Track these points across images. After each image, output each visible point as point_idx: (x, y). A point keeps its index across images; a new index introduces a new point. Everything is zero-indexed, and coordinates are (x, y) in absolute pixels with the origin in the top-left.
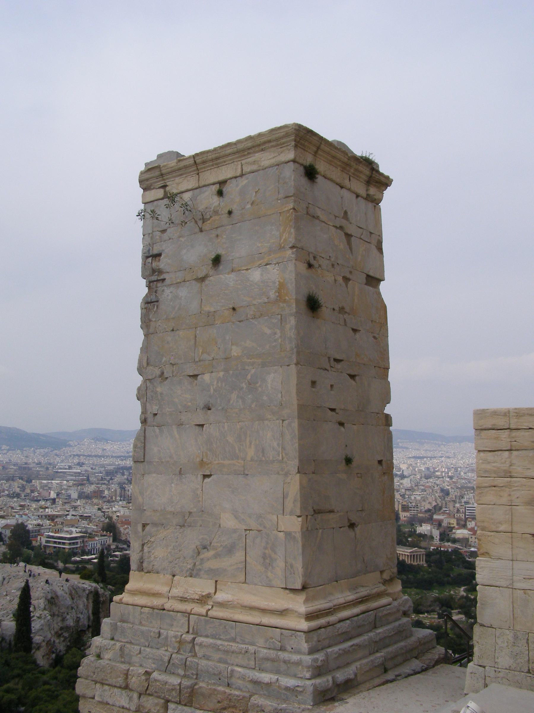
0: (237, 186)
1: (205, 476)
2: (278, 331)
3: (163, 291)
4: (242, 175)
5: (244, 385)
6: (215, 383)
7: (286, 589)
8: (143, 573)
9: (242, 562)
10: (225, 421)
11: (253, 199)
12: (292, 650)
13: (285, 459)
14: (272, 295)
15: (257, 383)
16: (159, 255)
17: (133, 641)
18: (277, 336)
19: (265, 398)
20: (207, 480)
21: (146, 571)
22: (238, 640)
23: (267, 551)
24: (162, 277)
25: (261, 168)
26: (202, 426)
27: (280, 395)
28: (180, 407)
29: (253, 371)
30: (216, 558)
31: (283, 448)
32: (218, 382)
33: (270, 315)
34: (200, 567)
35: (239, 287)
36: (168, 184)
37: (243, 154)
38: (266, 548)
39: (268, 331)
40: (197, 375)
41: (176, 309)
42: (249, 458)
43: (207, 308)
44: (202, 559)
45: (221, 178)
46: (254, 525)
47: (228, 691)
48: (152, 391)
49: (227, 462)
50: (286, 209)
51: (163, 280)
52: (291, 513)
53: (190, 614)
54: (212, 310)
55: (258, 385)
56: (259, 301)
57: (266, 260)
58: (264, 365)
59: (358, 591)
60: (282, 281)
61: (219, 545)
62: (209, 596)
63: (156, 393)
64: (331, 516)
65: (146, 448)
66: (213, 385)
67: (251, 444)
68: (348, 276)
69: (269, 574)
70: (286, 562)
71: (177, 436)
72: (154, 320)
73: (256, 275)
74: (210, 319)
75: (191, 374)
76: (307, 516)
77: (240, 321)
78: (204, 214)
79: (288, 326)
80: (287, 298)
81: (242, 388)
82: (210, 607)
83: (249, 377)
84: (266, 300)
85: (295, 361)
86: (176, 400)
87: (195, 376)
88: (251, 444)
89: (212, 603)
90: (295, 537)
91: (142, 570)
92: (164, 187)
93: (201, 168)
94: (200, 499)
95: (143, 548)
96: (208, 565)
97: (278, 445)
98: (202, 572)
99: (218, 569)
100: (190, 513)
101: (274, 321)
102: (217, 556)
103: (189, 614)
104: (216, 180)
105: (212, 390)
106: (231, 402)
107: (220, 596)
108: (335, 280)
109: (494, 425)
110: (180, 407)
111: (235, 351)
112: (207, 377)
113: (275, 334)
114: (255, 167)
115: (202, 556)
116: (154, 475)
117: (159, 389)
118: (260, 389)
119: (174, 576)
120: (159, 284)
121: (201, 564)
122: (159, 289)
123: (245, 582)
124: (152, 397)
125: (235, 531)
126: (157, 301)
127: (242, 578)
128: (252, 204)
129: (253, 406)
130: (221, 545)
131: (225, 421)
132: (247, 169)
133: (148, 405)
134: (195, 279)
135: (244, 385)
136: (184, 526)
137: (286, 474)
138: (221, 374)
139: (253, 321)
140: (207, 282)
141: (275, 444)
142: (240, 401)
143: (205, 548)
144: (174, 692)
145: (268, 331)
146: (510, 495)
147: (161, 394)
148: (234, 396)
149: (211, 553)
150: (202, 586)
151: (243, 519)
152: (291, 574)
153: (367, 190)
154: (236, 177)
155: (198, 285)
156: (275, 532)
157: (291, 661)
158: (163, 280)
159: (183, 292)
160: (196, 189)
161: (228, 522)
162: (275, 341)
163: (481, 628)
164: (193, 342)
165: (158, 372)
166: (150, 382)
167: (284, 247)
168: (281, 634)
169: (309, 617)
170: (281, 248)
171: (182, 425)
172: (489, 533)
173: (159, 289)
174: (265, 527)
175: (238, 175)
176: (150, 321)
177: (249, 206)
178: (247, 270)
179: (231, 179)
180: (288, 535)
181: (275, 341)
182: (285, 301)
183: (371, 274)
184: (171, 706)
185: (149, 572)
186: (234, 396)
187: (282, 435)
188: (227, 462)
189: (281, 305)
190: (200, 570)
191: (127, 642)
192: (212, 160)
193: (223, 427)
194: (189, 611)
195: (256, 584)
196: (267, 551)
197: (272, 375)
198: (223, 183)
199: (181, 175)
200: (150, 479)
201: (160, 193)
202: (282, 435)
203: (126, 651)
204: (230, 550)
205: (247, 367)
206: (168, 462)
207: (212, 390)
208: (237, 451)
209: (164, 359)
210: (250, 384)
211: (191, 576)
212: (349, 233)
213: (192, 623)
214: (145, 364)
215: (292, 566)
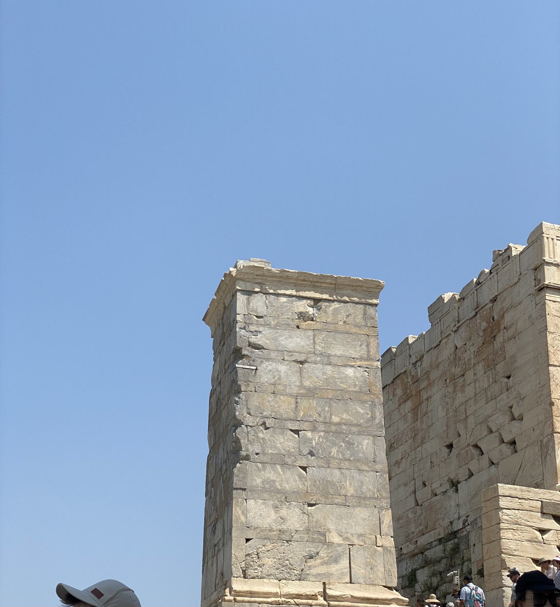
1: (310, 505)
6: (317, 439)
7: (385, 587)
9: (347, 568)
11: (345, 319)
19: (361, 455)
20: (310, 508)
23: (368, 560)
30: (323, 565)
34: (308, 572)
38: (368, 558)
39: (362, 411)
41: (276, 378)
43: (307, 383)
44: (310, 567)
46: (356, 541)
48: (254, 435)
52: (387, 535)
55: (355, 446)
56: (354, 390)
61: (325, 555)
63: (258, 437)
66: (315, 440)
69: (371, 576)
73: (350, 372)
81: (342, 446)
86: (279, 445)
87: (297, 432)
90: (390, 551)
96: (314, 571)
100: (297, 531)
106: (332, 454)
112: (309, 434)
113: (368, 414)
117: (261, 435)
119: (279, 581)
123: (351, 582)
125: (340, 545)
127: (348, 580)
128: (345, 322)
130: (327, 556)
136: (291, 541)
137: (381, 508)
140: (306, 365)
142: (340, 454)
143: (311, 557)
145: (362, 411)
147: (263, 439)
148: (334, 451)
149: (319, 561)
152: (389, 576)
159: (283, 368)
164: (293, 406)
174: (365, 543)
182: (374, 394)
185: (253, 578)
189: (372, 396)
190: (308, 574)
196: (368, 560)
197: (366, 441)
198: (320, 300)
200: (251, 502)
204: (336, 560)
215: (389, 570)
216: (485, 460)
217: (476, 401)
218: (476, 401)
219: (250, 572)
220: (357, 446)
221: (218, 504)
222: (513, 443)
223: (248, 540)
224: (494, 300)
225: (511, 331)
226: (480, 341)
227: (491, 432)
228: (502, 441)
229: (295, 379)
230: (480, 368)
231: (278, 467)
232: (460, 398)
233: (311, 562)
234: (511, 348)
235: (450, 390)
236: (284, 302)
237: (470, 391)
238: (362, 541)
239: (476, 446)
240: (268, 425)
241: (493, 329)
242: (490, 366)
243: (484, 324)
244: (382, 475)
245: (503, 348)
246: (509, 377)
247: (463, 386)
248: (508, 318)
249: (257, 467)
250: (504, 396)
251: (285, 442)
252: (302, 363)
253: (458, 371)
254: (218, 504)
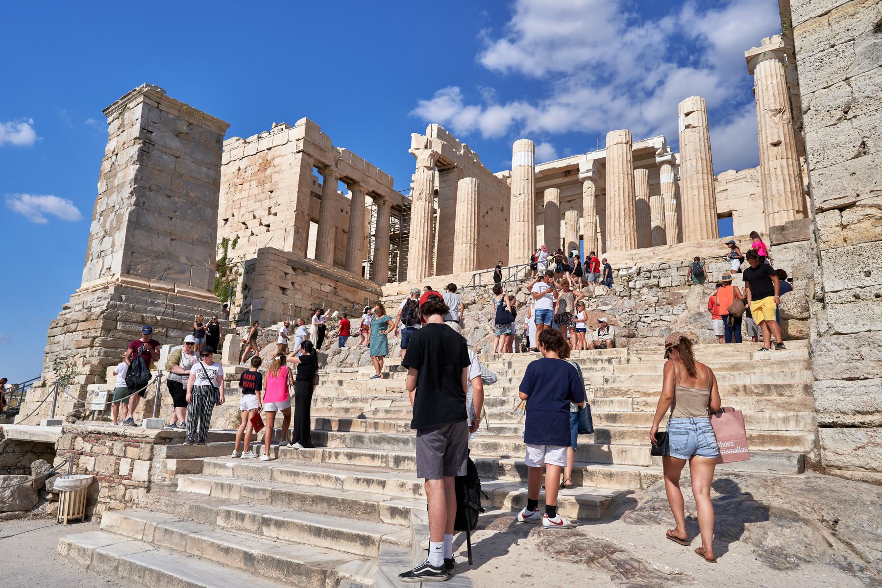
1: (172, 240)
74: (180, 176)
92: (158, 103)
102: (176, 273)
103: (167, 295)
111: (192, 194)
112: (177, 199)
117: (148, 193)
149: (171, 272)
159: (165, 157)
186: (190, 211)
201: (156, 105)
204: (183, 272)
214: (139, 177)
216: (248, 232)
217: (248, 200)
218: (248, 200)
219: (131, 272)
221: (108, 226)
222: (268, 226)
223: (132, 253)
224: (269, 149)
225: (277, 169)
226: (257, 169)
227: (254, 217)
228: (261, 224)
229: (172, 166)
230: (254, 183)
231: (156, 214)
232: (238, 196)
233: (168, 272)
234: (275, 177)
235: (232, 190)
237: (245, 194)
239: (244, 223)
241: (265, 165)
242: (261, 183)
243: (261, 161)
245: (271, 176)
246: (271, 192)
247: (241, 190)
248: (276, 162)
250: (267, 201)
251: (161, 201)
252: (177, 157)
253: (239, 181)
254: (108, 226)
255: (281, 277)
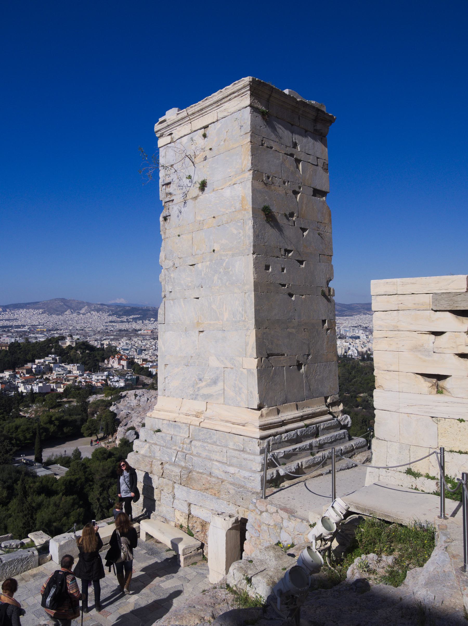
0: (215, 129)
2: (241, 231)
3: (173, 208)
4: (217, 120)
5: (221, 270)
8: (165, 397)
10: (211, 295)
12: (250, 451)
13: (247, 319)
14: (238, 205)
15: (229, 268)
16: (169, 183)
17: (157, 443)
18: (241, 235)
19: (234, 278)
20: (201, 334)
21: (167, 396)
22: (218, 443)
24: (172, 199)
25: (229, 114)
26: (198, 298)
27: (243, 276)
28: (184, 287)
29: (227, 260)
30: (207, 387)
31: (246, 312)
32: (206, 269)
33: (236, 220)
34: (197, 393)
35: (218, 201)
36: (173, 132)
37: (217, 105)
39: (235, 232)
40: (194, 265)
42: (225, 320)
43: (199, 218)
44: (199, 388)
45: (204, 124)
46: (229, 365)
47: (209, 478)
48: (169, 277)
49: (212, 322)
50: (245, 142)
51: (173, 200)
52: (251, 356)
53: (190, 424)
54: (202, 219)
55: (230, 270)
56: (230, 211)
57: (233, 182)
58: (233, 255)
59: (304, 410)
60: (243, 195)
61: (208, 378)
62: (202, 413)
64: (282, 358)
65: (166, 314)
67: (226, 310)
68: (297, 190)
70: (248, 390)
71: (184, 306)
72: (168, 228)
73: (227, 193)
75: (191, 264)
76: (262, 358)
77: (218, 226)
78: (195, 151)
79: (247, 228)
80: (247, 207)
81: (220, 273)
82: (203, 420)
83: (224, 264)
84: (234, 210)
85: (252, 252)
86: (182, 282)
88: (226, 310)
89: (203, 418)
90: (253, 372)
91: (165, 396)
93: (192, 119)
94: (197, 347)
95: (165, 381)
96: (202, 392)
97: (242, 310)
98: (199, 396)
99: (208, 394)
100: (192, 357)
101: (239, 224)
104: (202, 126)
105: (203, 275)
106: (214, 282)
107: (209, 413)
108: (286, 193)
109: (386, 292)
110: (184, 287)
112: (199, 266)
114: (225, 114)
115: (198, 386)
116: (171, 332)
117: (172, 275)
118: (231, 272)
120: (170, 204)
121: (198, 391)
122: (170, 207)
123: (224, 404)
124: (168, 280)
125: (218, 368)
126: (170, 216)
127: (222, 401)
129: (227, 284)
131: (211, 295)
132: (221, 116)
133: (166, 285)
134: (191, 199)
135: (221, 270)
136: (188, 365)
137: (248, 329)
138: (208, 263)
139: (226, 225)
140: (198, 199)
141: (240, 309)
144: (177, 477)
145: (235, 232)
146: (397, 344)
147: (174, 278)
148: (216, 278)
149: (204, 384)
150: (199, 405)
151: (222, 361)
152: (251, 398)
153: (314, 126)
154: (214, 123)
155: (194, 202)
156: (242, 369)
157: (248, 459)
158: (173, 200)
160: (190, 134)
161: (214, 362)
162: (240, 238)
163: (377, 441)
164: (191, 242)
165: (171, 264)
166: (167, 270)
167: (244, 171)
168: (243, 440)
169: (263, 428)
170: (243, 172)
171: (186, 298)
172: (383, 372)
173: (170, 207)
174: (235, 366)
175: (215, 121)
176: (166, 229)
177: (222, 143)
178: (222, 189)
179: (211, 124)
180: (249, 371)
181: (240, 238)
183: (318, 188)
184: (176, 486)
185: (168, 397)
187: (245, 303)
188: (212, 322)
189: (243, 212)
190: (197, 395)
191: (153, 443)
192: (198, 111)
193: (210, 299)
194: (189, 423)
195: (230, 405)
196: (236, 382)
198: (206, 127)
199: (180, 124)
202: (245, 303)
203: (152, 449)
204: (215, 382)
205: (223, 258)
206: (178, 323)
207: (203, 275)
208: (218, 315)
209: (175, 255)
210: (225, 269)
211: (192, 399)
212: (299, 158)
213: (191, 431)
215: (251, 393)
220: (231, 270)
223: (166, 365)
236: (186, 143)
238: (232, 364)
240: (176, 266)
244: (249, 295)
249: (170, 304)
255: (416, 349)
